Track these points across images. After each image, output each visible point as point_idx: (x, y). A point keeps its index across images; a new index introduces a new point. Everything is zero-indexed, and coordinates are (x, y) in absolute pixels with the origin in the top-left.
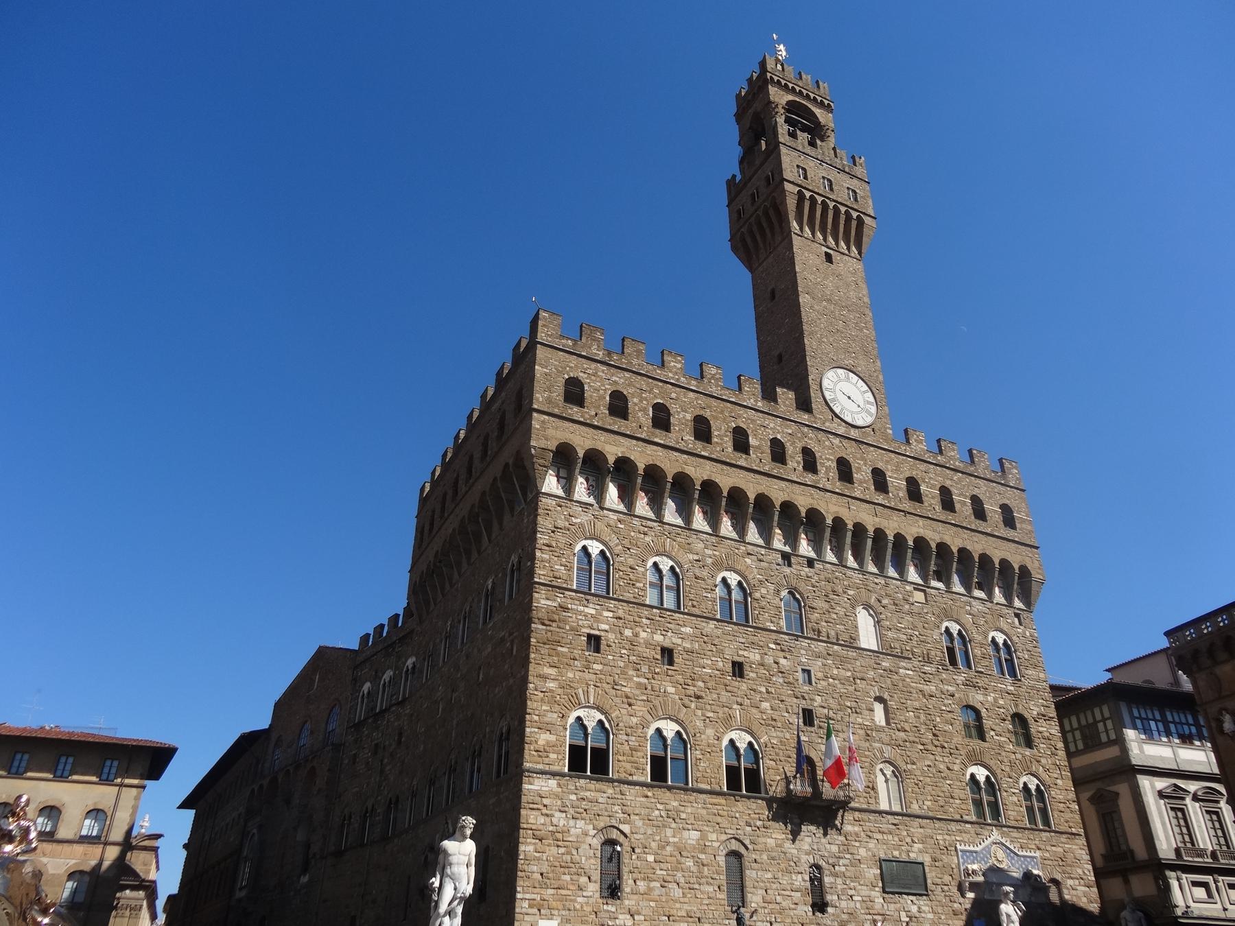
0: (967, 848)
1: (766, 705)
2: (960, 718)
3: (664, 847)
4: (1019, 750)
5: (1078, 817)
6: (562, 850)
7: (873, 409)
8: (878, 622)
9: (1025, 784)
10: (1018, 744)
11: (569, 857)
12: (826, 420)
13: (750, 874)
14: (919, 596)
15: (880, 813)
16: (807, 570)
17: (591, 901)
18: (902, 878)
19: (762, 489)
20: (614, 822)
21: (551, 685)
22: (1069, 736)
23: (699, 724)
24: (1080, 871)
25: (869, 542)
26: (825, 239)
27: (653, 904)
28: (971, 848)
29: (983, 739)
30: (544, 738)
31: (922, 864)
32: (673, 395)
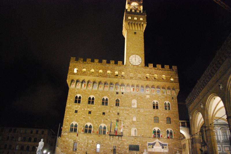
0: (150, 143)
2: (153, 119)
3: (85, 143)
7: (141, 61)
8: (137, 102)
11: (68, 145)
15: (131, 136)
16: (122, 94)
19: (112, 81)
21: (68, 119)
23: (95, 123)
24: (178, 146)
25: (135, 88)
26: (135, 29)
28: (151, 143)
30: (65, 127)
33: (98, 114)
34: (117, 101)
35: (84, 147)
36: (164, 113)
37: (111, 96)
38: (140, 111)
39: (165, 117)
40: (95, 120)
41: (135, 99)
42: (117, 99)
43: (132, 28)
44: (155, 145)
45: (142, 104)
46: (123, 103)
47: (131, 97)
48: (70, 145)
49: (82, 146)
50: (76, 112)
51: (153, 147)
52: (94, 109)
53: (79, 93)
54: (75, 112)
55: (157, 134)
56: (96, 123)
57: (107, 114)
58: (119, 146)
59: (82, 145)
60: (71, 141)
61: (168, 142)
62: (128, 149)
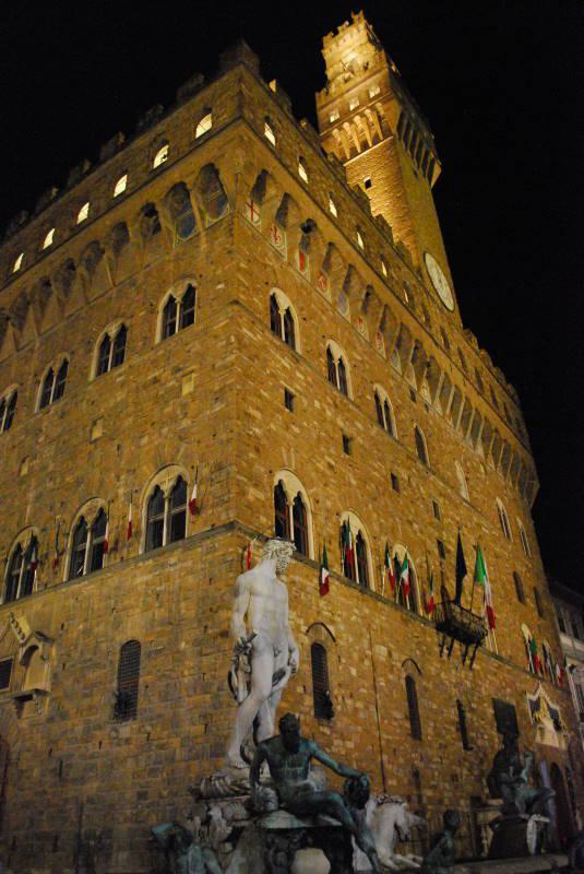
3: (362, 660)
8: (467, 479)
13: (422, 702)
17: (308, 717)
20: (320, 619)
21: (257, 430)
23: (376, 528)
27: (359, 729)
33: (376, 473)
40: (375, 510)
52: (359, 432)
56: (381, 532)
59: (354, 672)
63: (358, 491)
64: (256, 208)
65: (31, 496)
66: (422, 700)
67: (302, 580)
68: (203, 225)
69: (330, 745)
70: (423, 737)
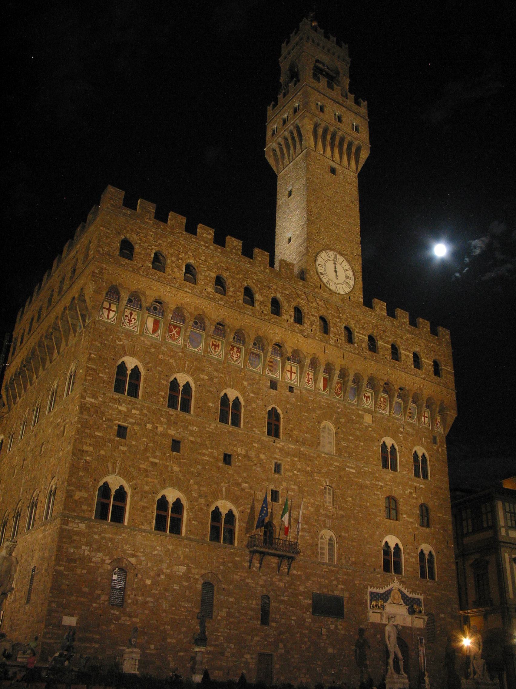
1: (244, 485)
2: (383, 504)
3: (159, 575)
4: (422, 528)
5: (454, 575)
6: (85, 571)
7: (351, 283)
9: (422, 551)
10: (422, 525)
12: (316, 287)
13: (219, 598)
14: (368, 419)
16: (289, 393)
18: (328, 606)
19: (261, 334)
21: (88, 458)
22: (465, 523)
25: (336, 379)
27: (147, 612)
29: (397, 520)
30: (78, 495)
31: (343, 598)
32: (203, 258)
34: (273, 415)
35: (153, 591)
36: (411, 487)
37: (253, 392)
38: (347, 469)
39: (414, 501)
40: (196, 483)
41: (330, 419)
42: (273, 408)
43: (324, 151)
44: (390, 600)
45: (351, 445)
46: (293, 430)
47: (318, 412)
48: (99, 579)
49: (146, 586)
50: (122, 432)
51: (383, 607)
52: (191, 433)
53: (133, 354)
54: (118, 437)
55: (391, 561)
56: (200, 496)
57: (239, 461)
58: (282, 598)
59: (148, 582)
60: (103, 561)
61: (424, 593)
62: (311, 610)
63: (180, 474)
64: (114, 308)
65: (23, 481)
66: (218, 596)
67: (111, 536)
68: (84, 325)
69: (117, 618)
70: (213, 617)
